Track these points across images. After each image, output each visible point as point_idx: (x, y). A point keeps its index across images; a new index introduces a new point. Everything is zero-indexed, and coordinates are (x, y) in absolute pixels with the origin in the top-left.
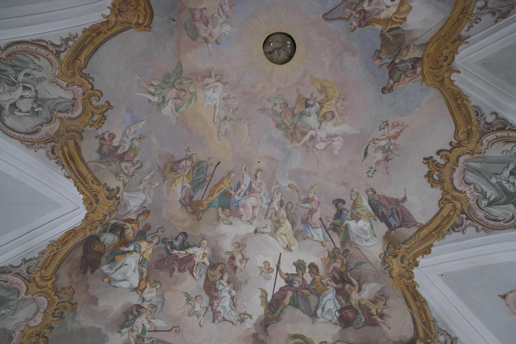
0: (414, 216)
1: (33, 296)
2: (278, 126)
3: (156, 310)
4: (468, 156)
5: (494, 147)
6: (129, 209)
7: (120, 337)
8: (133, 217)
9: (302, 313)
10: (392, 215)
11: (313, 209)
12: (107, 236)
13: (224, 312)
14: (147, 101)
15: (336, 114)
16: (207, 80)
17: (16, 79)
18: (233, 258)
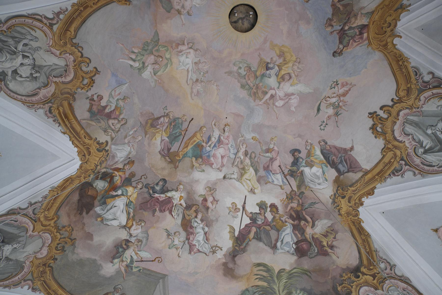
0: (360, 162)
1: (39, 233)
2: (243, 86)
3: (141, 244)
4: (407, 110)
5: (430, 102)
6: (116, 159)
7: (113, 266)
8: (120, 166)
9: (264, 246)
10: (341, 162)
11: (273, 158)
12: (99, 183)
13: (199, 245)
14: (130, 66)
15: (293, 75)
16: (181, 48)
17: (16, 48)
18: (205, 200)
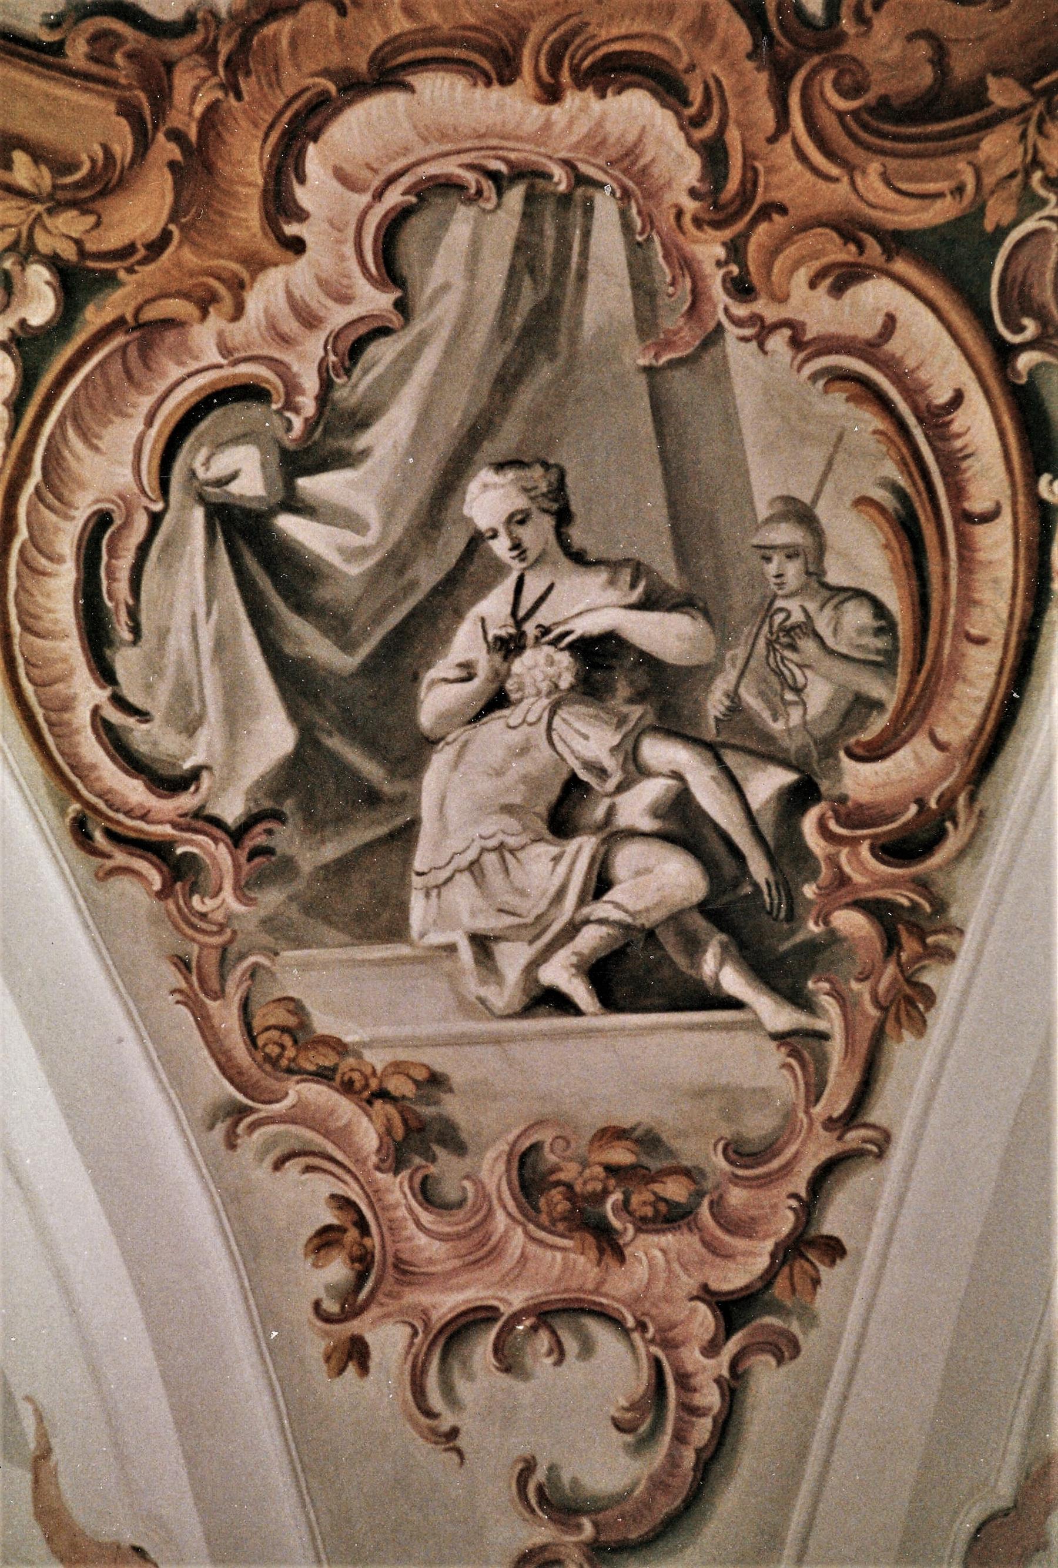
4: (690, 169)
5: (837, 404)
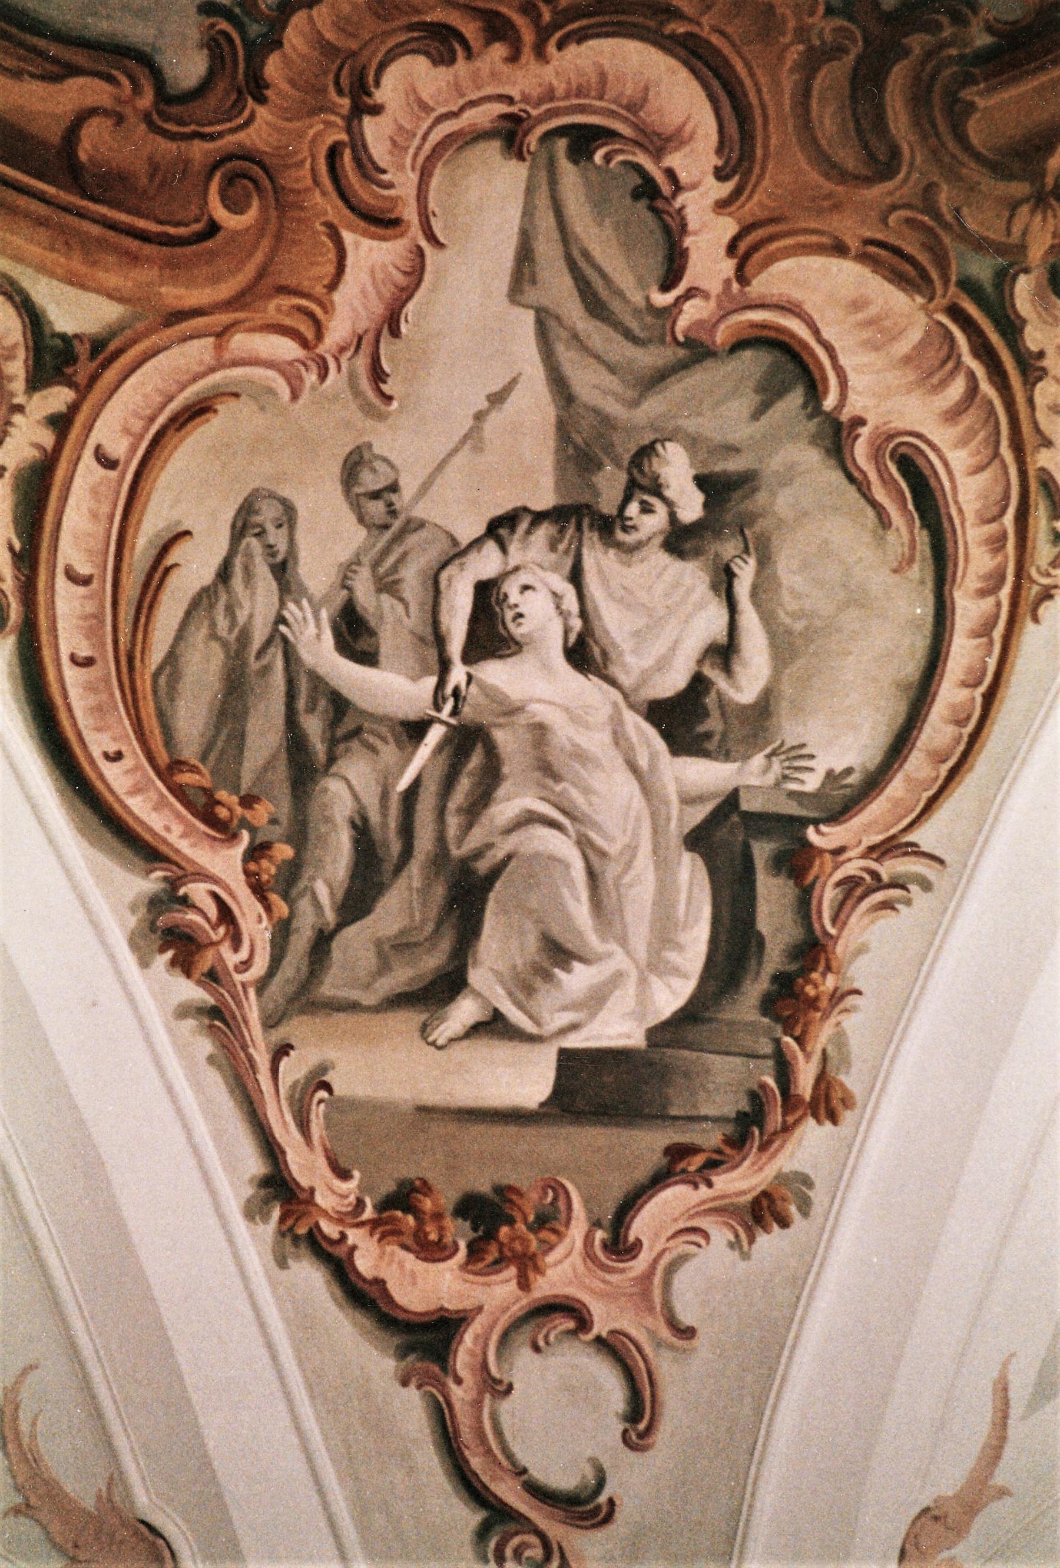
17: (415, 730)
